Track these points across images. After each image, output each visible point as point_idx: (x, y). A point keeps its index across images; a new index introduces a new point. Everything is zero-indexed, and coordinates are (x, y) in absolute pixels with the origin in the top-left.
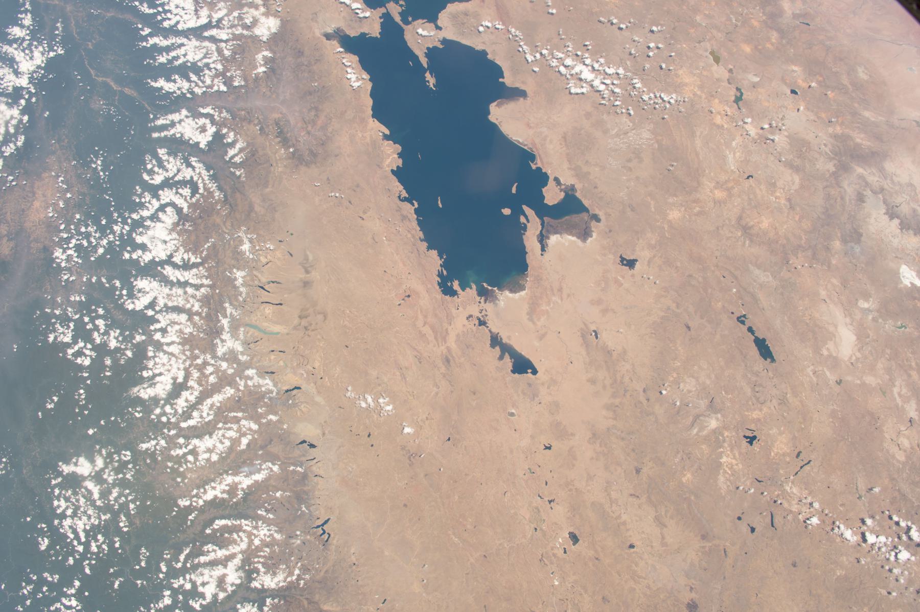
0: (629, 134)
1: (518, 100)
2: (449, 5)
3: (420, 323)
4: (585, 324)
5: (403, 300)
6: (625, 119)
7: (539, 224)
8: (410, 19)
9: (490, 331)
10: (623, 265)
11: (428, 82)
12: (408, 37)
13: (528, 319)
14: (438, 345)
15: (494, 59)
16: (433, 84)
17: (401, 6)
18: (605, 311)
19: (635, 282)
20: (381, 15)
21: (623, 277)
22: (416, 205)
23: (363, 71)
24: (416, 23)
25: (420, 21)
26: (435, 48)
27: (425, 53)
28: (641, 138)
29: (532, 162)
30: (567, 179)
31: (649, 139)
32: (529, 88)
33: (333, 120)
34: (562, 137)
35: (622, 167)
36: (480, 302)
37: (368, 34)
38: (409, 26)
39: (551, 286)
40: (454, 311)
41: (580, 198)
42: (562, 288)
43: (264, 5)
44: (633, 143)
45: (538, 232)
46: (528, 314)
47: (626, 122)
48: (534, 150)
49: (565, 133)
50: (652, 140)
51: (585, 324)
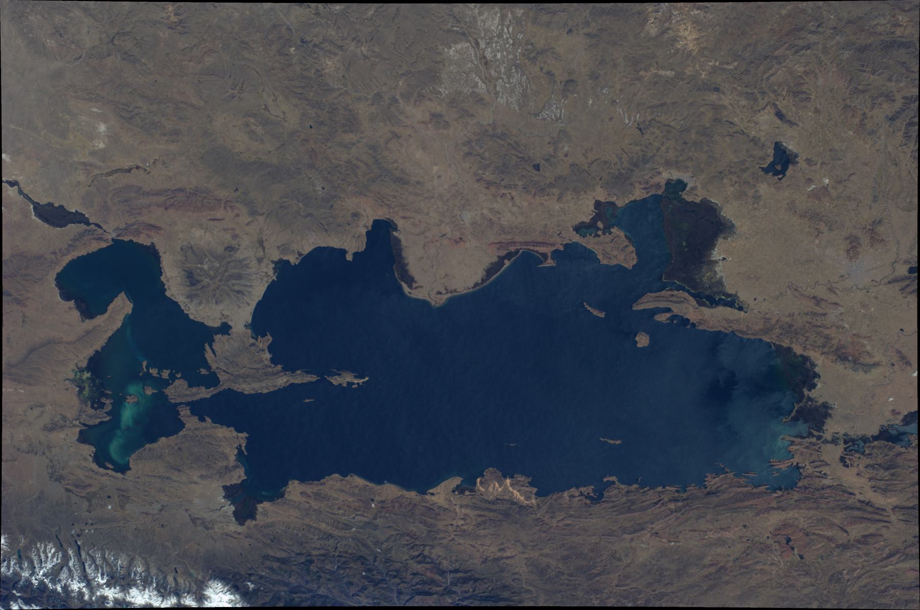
0: (489, 55)
1: (398, 241)
2: (168, 294)
3: (842, 538)
4: (896, 280)
5: (793, 549)
6: (451, 52)
7: (675, 292)
8: (204, 372)
9: (875, 438)
10: (783, 172)
11: (350, 384)
12: (247, 388)
13: (866, 372)
14: (887, 522)
15: (300, 254)
16: (356, 377)
17: (173, 378)
18: (875, 238)
19: (823, 163)
20: (196, 419)
21: (809, 181)
22: (613, 479)
23: (322, 481)
24: (214, 366)
25: (209, 355)
26: (271, 349)
27: (285, 369)
28: (500, 36)
29: (541, 263)
30: (585, 211)
31: (503, 18)
32: (370, 213)
33: (426, 553)
34: (487, 188)
35: (565, 100)
36: (819, 438)
37: (239, 448)
38: (222, 377)
39: (807, 314)
40: (827, 482)
41: (627, 202)
42: (814, 298)
43: (178, 595)
44: (511, 57)
45: (693, 301)
46: (855, 370)
47: (457, 51)
48: (512, 249)
49: (478, 181)
50: (507, 16)
51: (896, 280)
